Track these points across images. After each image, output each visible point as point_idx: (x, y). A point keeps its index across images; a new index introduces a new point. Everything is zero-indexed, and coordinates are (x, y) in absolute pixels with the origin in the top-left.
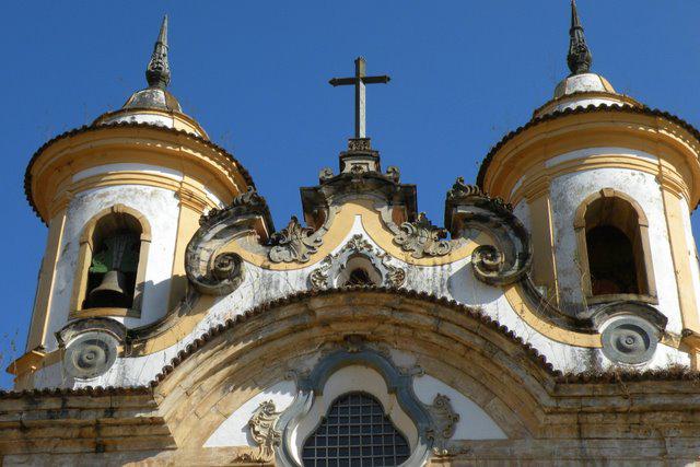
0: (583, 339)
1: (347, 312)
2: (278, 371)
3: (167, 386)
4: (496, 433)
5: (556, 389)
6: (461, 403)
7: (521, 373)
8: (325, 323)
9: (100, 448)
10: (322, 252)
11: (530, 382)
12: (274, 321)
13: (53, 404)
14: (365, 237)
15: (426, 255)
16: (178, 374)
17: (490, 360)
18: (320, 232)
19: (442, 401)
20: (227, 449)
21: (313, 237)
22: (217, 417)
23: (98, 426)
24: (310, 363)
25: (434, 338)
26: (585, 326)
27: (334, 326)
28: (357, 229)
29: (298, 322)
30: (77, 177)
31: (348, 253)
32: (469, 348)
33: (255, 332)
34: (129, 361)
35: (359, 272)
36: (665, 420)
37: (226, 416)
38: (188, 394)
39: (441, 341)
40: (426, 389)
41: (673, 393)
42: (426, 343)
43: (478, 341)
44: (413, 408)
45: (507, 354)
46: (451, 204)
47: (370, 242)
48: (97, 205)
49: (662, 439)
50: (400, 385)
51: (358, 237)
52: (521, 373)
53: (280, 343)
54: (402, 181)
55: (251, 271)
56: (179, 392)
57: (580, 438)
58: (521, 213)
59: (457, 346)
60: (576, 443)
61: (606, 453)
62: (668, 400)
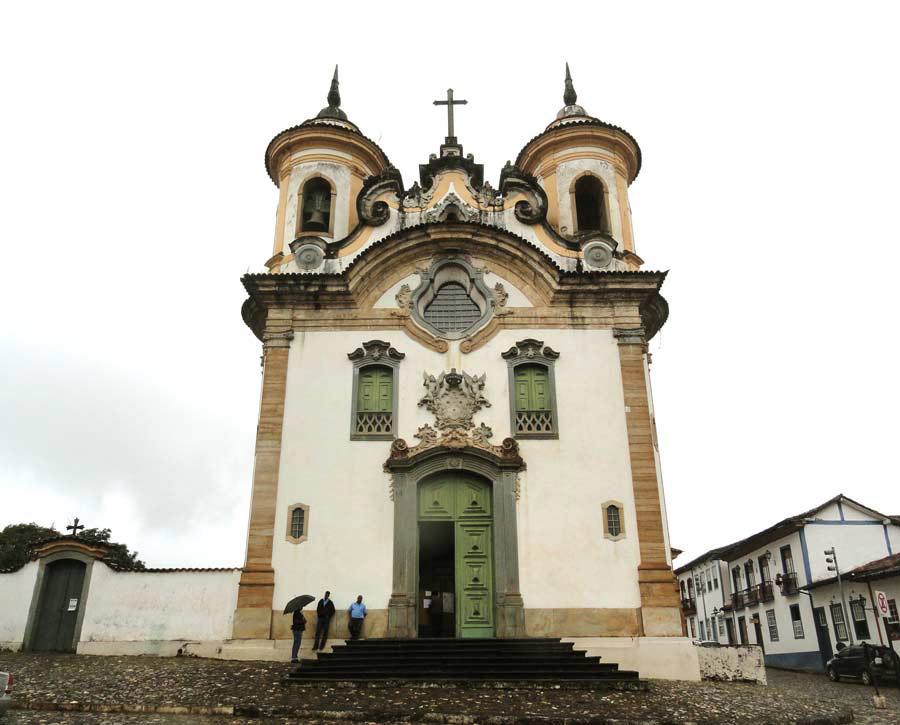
0: (573, 253)
1: (448, 236)
2: (411, 268)
3: (351, 275)
4: (530, 305)
5: (561, 279)
6: (508, 287)
7: (542, 271)
8: (435, 241)
9: (318, 307)
10: (433, 203)
11: (547, 276)
12: (408, 240)
13: (292, 282)
14: (456, 194)
15: (490, 205)
16: (357, 268)
17: (525, 263)
18: (431, 191)
19: (499, 287)
20: (385, 310)
21: (427, 194)
22: (379, 293)
23: (316, 295)
25: (495, 252)
27: (441, 244)
28: (452, 189)
29: (421, 241)
30: (293, 157)
31: (448, 203)
32: (515, 257)
33: (396, 246)
34: (330, 261)
36: (615, 297)
37: (384, 292)
38: (363, 279)
39: (500, 253)
40: (490, 281)
41: (620, 282)
42: (490, 255)
43: (519, 254)
45: (535, 261)
46: (505, 174)
47: (459, 197)
49: (613, 307)
51: (452, 194)
52: (542, 271)
53: (411, 253)
54: (476, 162)
55: (394, 210)
56: (358, 278)
57: (571, 307)
58: (541, 183)
59: (507, 257)
60: (569, 309)
61: (584, 314)
62: (617, 286)
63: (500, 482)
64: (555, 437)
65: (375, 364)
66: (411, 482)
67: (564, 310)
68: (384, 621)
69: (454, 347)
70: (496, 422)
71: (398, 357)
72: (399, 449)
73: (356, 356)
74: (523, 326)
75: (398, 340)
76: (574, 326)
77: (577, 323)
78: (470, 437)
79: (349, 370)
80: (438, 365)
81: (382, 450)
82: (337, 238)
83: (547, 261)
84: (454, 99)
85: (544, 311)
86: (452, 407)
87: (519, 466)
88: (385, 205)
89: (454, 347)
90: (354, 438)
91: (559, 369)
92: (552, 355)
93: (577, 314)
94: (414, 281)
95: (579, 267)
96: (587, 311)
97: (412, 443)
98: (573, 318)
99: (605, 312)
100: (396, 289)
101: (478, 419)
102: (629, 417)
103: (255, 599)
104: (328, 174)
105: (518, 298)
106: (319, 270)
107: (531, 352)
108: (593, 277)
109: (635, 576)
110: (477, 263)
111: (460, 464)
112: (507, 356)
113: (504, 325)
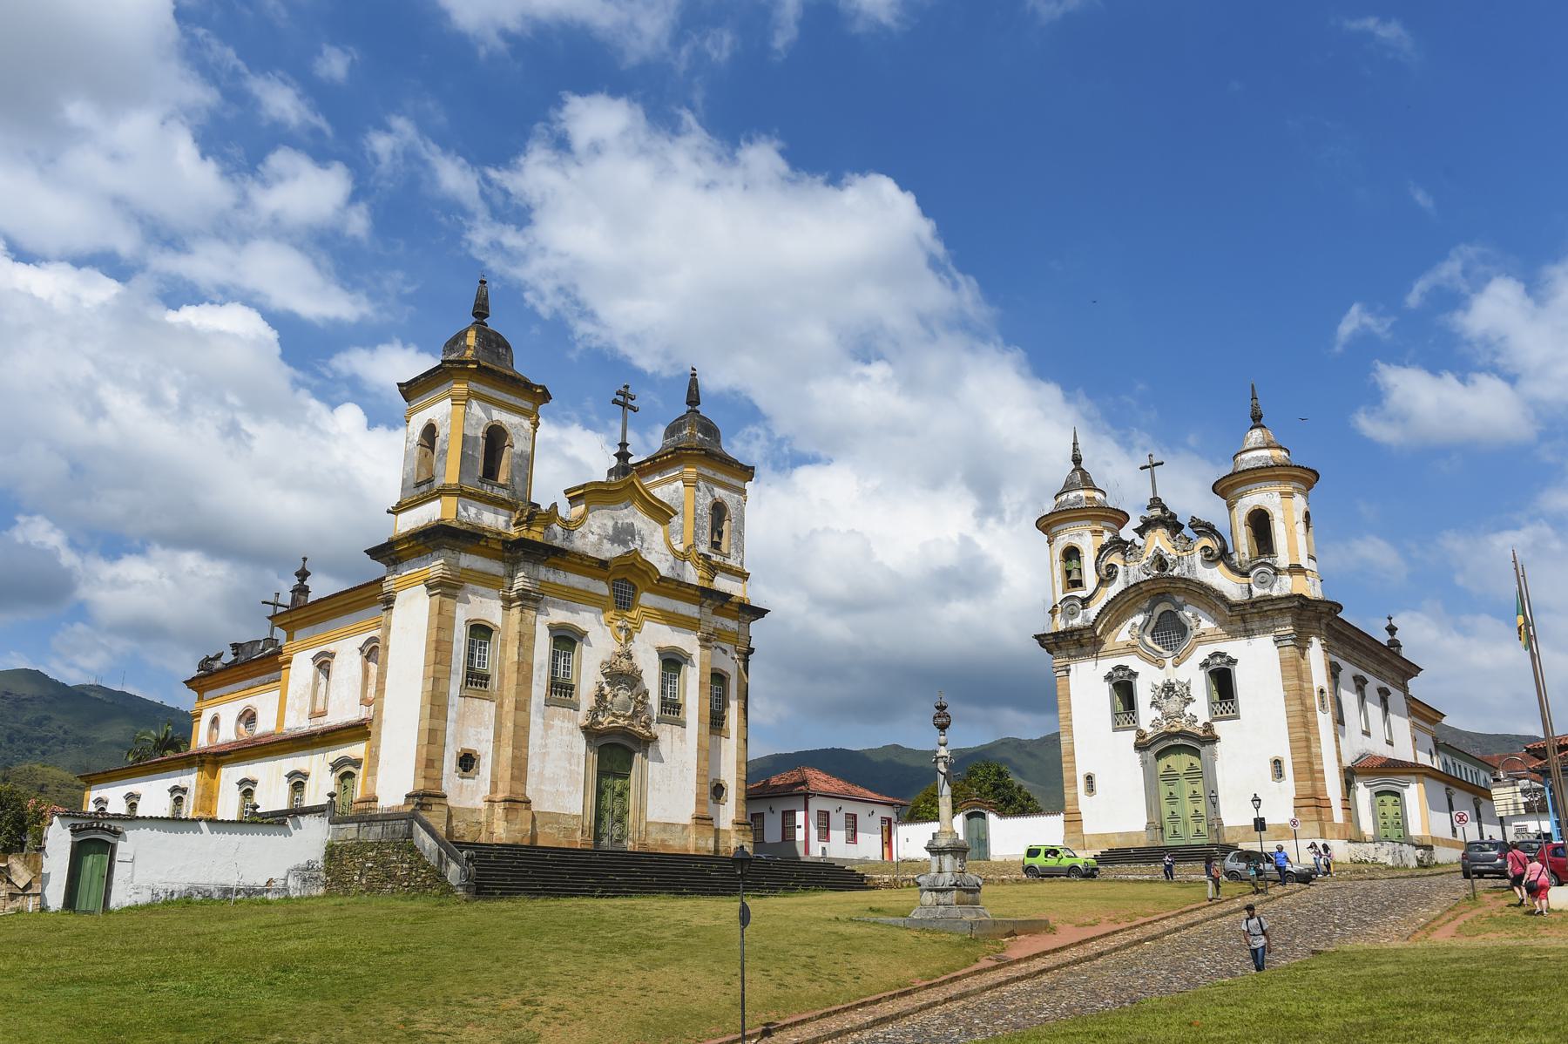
0: (1245, 580)
26: (1246, 575)
28: (1158, 543)
35: (1161, 562)
40: (1187, 613)
55: (1121, 568)
63: (1204, 750)
64: (1237, 717)
66: (1151, 754)
68: (1145, 837)
69: (1169, 662)
71: (1135, 675)
72: (1141, 735)
73: (1109, 678)
74: (1213, 641)
75: (1133, 662)
77: (1248, 633)
78: (1181, 724)
79: (1106, 687)
81: (1131, 736)
82: (1089, 591)
83: (1222, 598)
86: (1173, 705)
87: (1214, 739)
88: (1113, 566)
89: (1169, 662)
90: (1115, 730)
94: (1139, 619)
95: (1250, 590)
97: (1148, 730)
98: (1246, 631)
101: (1188, 710)
102: (1286, 699)
103: (1073, 828)
104: (1076, 542)
105: (1207, 624)
106: (1077, 622)
107: (1218, 660)
109: (1292, 803)
110: (1179, 599)
111: (1180, 741)
112: (1205, 665)
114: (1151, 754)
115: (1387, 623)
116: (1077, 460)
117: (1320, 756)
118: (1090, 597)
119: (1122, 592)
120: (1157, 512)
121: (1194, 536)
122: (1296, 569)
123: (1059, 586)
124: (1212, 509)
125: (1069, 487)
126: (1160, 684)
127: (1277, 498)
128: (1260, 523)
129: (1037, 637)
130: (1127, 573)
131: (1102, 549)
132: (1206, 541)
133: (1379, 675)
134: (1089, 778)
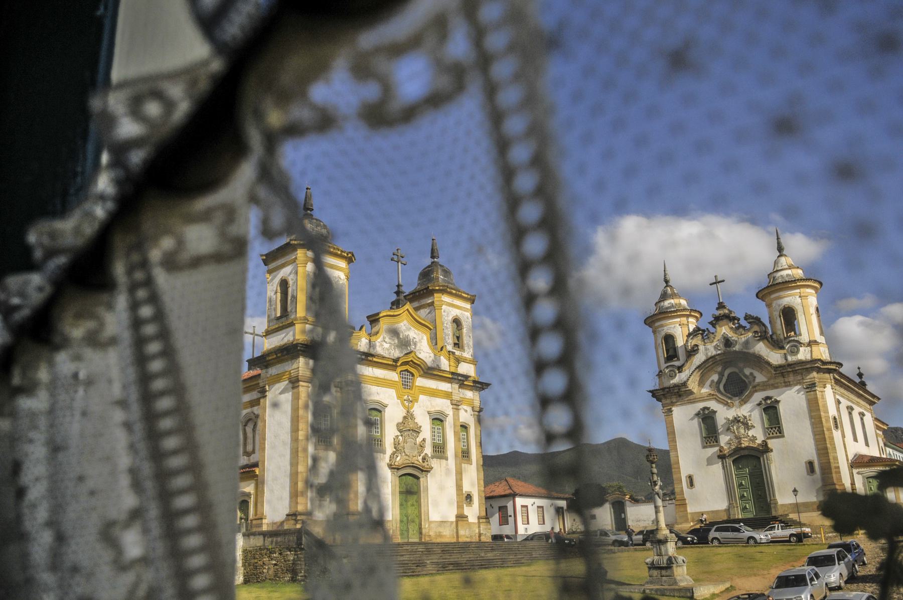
4: (765, 379)
6: (756, 373)
9: (680, 396)
10: (717, 338)
19: (751, 374)
24: (719, 369)
26: (782, 348)
28: (724, 331)
35: (727, 342)
40: (747, 371)
44: (746, 376)
48: (663, 334)
50: (742, 371)
55: (701, 348)
64: (783, 436)
65: (707, 418)
67: (781, 380)
70: (757, 434)
71: (715, 412)
73: (698, 414)
74: (764, 390)
75: (713, 405)
76: (786, 386)
77: (788, 385)
80: (731, 414)
84: (719, 280)
85: (772, 382)
88: (697, 346)
91: (782, 408)
92: (777, 402)
93: (786, 380)
94: (715, 377)
96: (791, 378)
98: (785, 382)
99: (799, 377)
100: (708, 383)
104: (671, 331)
105: (760, 378)
106: (676, 380)
108: (790, 365)
110: (741, 365)
111: (746, 452)
113: (756, 391)
114: (729, 461)
115: (858, 372)
116: (667, 281)
117: (836, 458)
118: (683, 365)
119: (704, 362)
120: (721, 312)
121: (748, 326)
122: (812, 343)
123: (662, 360)
124: (760, 310)
125: (664, 296)
126: (731, 418)
127: (799, 300)
128: (789, 315)
129: (650, 391)
130: (706, 349)
131: (689, 335)
132: (756, 328)
133: (858, 404)
134: (690, 479)
